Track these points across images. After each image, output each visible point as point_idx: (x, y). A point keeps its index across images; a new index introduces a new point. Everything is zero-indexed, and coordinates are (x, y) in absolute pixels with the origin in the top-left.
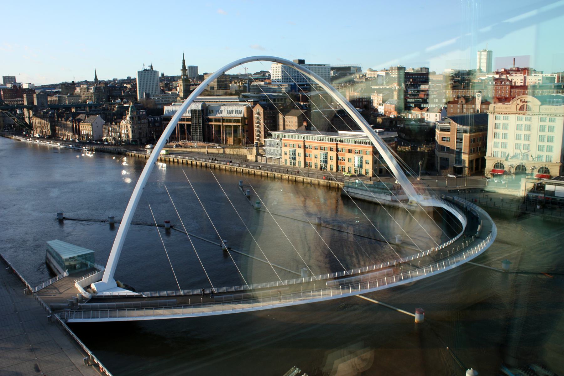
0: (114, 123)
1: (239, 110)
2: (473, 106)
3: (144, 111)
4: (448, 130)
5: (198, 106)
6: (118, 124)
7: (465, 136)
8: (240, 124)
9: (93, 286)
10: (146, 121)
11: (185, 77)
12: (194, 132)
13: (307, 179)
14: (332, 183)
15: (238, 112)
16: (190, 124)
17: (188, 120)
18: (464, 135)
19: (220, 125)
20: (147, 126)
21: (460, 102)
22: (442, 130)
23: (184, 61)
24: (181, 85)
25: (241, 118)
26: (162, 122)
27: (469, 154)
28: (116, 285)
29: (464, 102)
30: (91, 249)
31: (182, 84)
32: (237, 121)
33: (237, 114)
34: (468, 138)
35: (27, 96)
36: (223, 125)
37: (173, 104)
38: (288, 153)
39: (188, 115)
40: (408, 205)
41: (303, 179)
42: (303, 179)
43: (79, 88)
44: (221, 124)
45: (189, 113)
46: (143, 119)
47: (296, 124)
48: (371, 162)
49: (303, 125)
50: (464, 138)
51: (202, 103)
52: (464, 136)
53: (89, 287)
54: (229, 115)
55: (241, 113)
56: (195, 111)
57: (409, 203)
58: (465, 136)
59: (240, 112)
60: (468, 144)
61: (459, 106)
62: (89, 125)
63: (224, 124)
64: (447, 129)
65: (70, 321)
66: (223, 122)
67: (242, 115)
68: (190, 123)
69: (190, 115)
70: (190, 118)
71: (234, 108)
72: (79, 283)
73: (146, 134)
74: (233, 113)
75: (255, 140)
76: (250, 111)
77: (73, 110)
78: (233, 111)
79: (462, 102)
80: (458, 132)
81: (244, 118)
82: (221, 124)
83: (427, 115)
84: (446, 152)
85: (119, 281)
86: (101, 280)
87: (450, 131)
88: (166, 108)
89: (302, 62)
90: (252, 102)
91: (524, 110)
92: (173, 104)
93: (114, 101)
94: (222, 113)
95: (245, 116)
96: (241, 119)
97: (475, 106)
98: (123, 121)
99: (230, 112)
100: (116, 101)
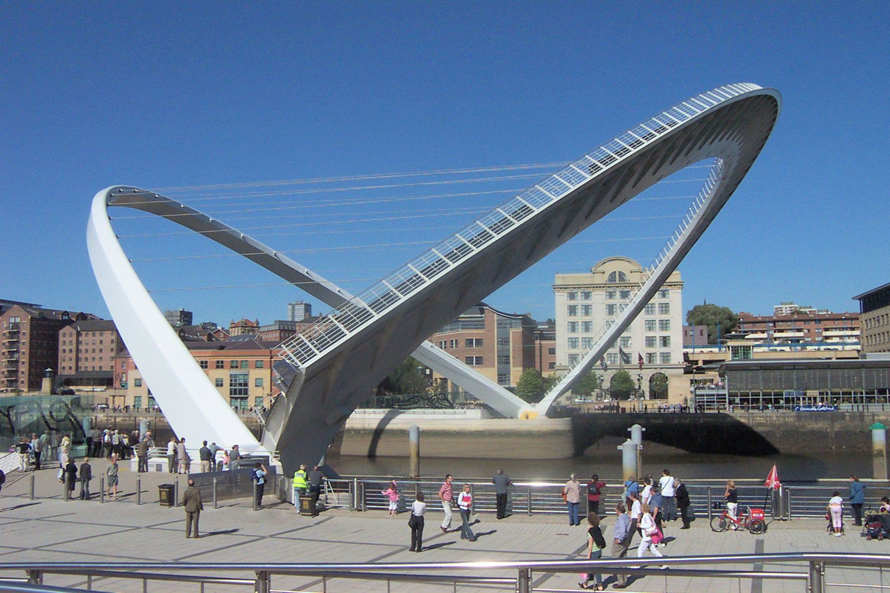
7: (513, 332)
34: (520, 335)
52: (511, 333)
58: (513, 332)
84: (473, 367)
87: (483, 328)
91: (615, 281)
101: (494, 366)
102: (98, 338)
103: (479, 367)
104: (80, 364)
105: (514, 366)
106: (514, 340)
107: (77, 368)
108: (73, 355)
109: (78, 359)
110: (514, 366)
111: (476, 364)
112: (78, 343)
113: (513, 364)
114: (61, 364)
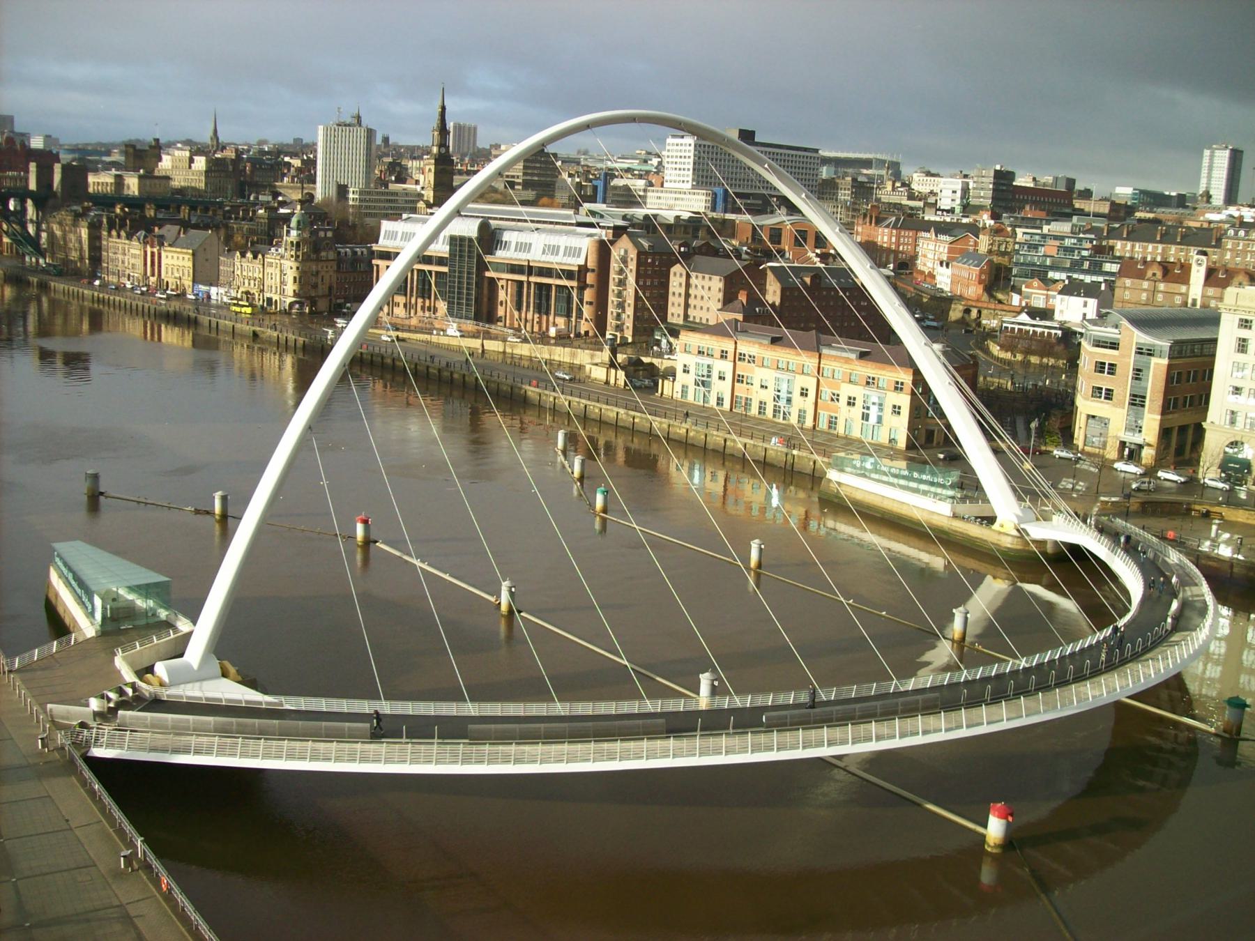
0: (249, 255)
1: (526, 244)
2: (1183, 289)
3: (329, 230)
4: (1114, 346)
5: (468, 228)
6: (260, 256)
7: (1156, 364)
8: (574, 284)
9: (161, 669)
10: (332, 255)
11: (443, 150)
12: (454, 293)
13: (734, 441)
14: (799, 456)
15: (571, 251)
16: (446, 273)
17: (441, 261)
18: (1154, 360)
19: (520, 283)
20: (335, 267)
21: (1150, 273)
22: (1099, 343)
23: (443, 108)
24: (430, 170)
25: (576, 269)
26: (374, 262)
27: (1163, 413)
28: (219, 672)
29: (1159, 274)
30: (159, 571)
31: (433, 168)
32: (569, 275)
33: (569, 256)
34: (1164, 369)
35: (37, 167)
36: (529, 283)
37: (405, 216)
38: (692, 370)
40: (994, 531)
41: (725, 441)
42: (725, 441)
43: (169, 157)
44: (523, 278)
45: (443, 243)
46: (324, 249)
47: (721, 296)
48: (905, 412)
49: (737, 298)
50: (1154, 368)
51: (480, 220)
53: (150, 669)
54: (544, 258)
55: (579, 256)
56: (462, 239)
57: (996, 526)
58: (1156, 364)
59: (575, 252)
60: (1161, 385)
61: (1145, 284)
63: (533, 279)
64: (1111, 343)
65: (98, 752)
66: (530, 274)
67: (582, 262)
68: (445, 269)
69: (447, 248)
70: (447, 256)
71: (563, 241)
72: (124, 658)
73: (330, 288)
74: (557, 254)
75: (608, 327)
76: (603, 250)
77: (150, 212)
78: (559, 247)
79: (1154, 274)
80: (1140, 351)
81: (583, 270)
82: (523, 278)
83: (1062, 300)
84: (1102, 402)
85: (226, 663)
86: (181, 655)
88: (386, 225)
89: (748, 136)
90: (609, 228)
92: (405, 216)
93: (119, 181)
94: (529, 251)
95: (588, 264)
96: (579, 271)
97: (1188, 289)
98: (273, 249)
100: (261, 198)
101: (1124, 408)
102: (707, 283)
103: (1108, 403)
104: (690, 312)
105: (1149, 412)
106: (1154, 376)
107: (686, 316)
108: (682, 300)
109: (687, 306)
110: (1149, 412)
111: (1106, 398)
112: (688, 285)
113: (1149, 408)
114: (671, 310)
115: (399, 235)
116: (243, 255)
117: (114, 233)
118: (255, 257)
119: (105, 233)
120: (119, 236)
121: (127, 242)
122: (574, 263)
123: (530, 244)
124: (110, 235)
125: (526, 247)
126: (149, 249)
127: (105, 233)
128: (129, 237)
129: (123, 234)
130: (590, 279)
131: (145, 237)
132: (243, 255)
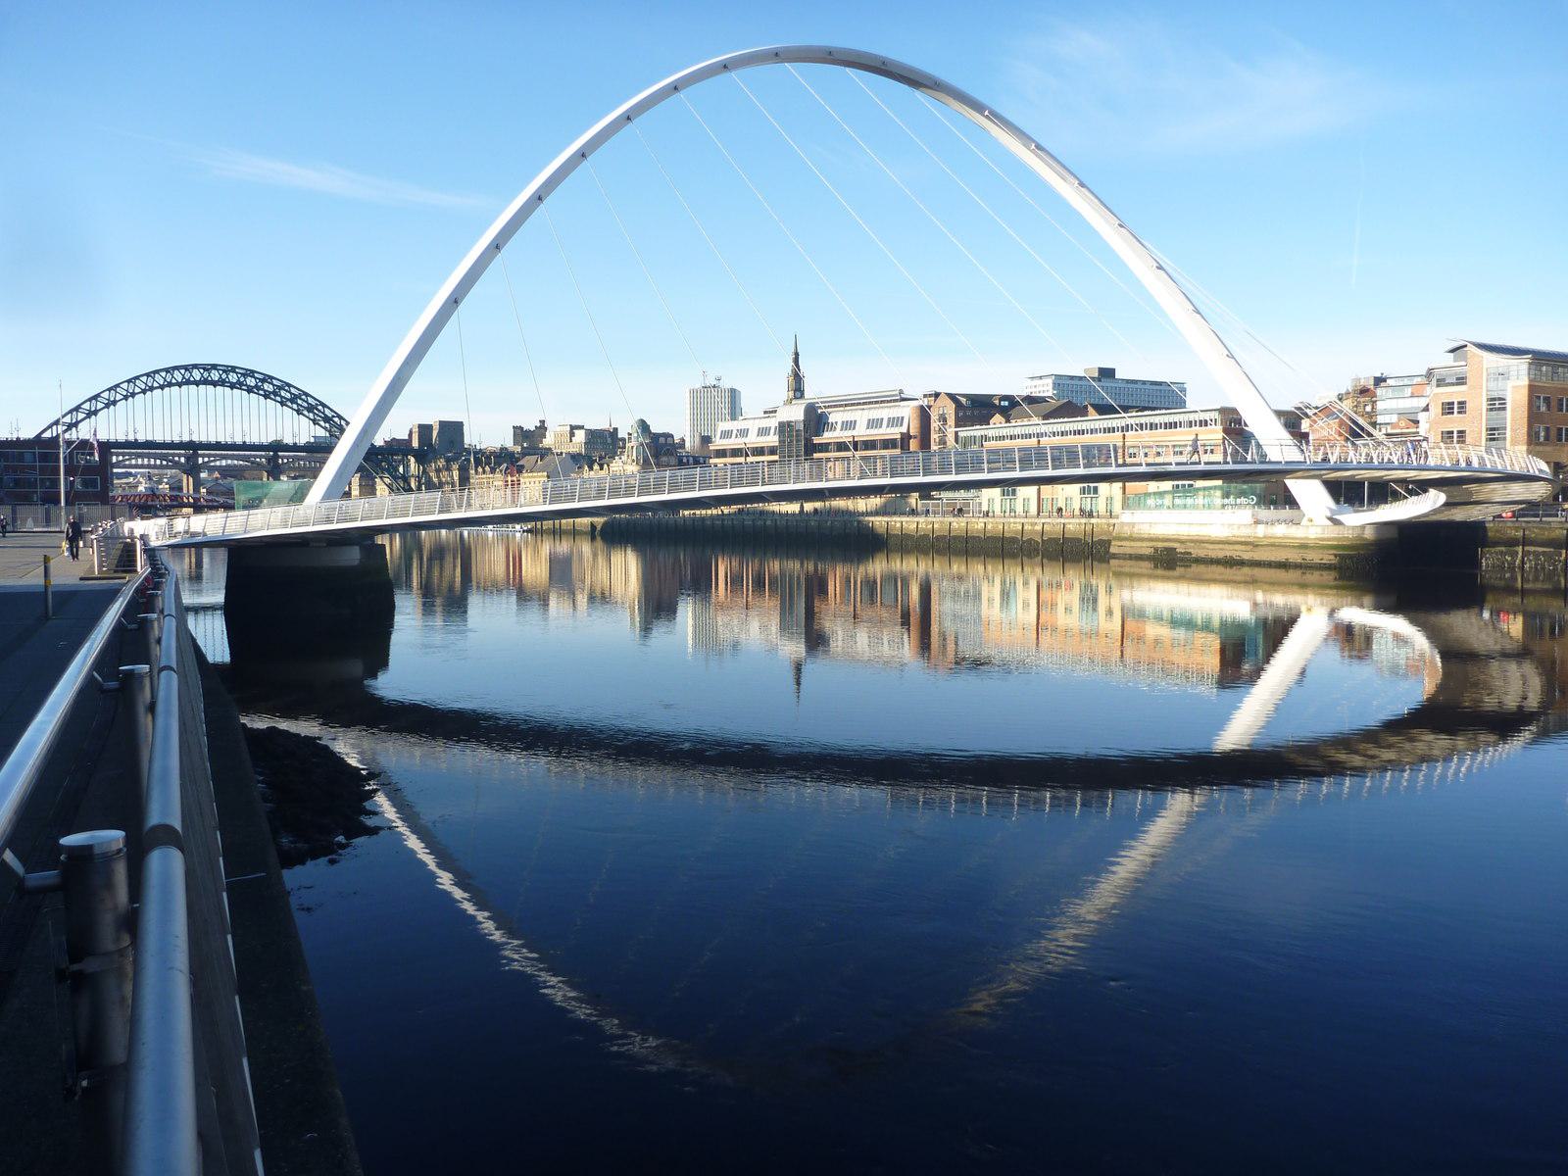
0: (596, 467)
15: (896, 421)
17: (772, 451)
25: (899, 436)
39: (772, 440)
45: (775, 434)
55: (901, 425)
62: (543, 476)
67: (904, 430)
69: (776, 438)
70: (777, 444)
74: (881, 427)
81: (906, 438)
94: (854, 428)
96: (902, 439)
99: (873, 423)
115: (735, 432)
116: (591, 469)
117: (480, 470)
118: (601, 469)
119: (472, 472)
120: (484, 472)
121: (491, 475)
122: (895, 433)
123: (855, 421)
124: (477, 472)
125: (850, 425)
126: (509, 479)
127: (472, 472)
128: (493, 471)
129: (487, 468)
130: (913, 445)
131: (507, 468)
132: (591, 469)
